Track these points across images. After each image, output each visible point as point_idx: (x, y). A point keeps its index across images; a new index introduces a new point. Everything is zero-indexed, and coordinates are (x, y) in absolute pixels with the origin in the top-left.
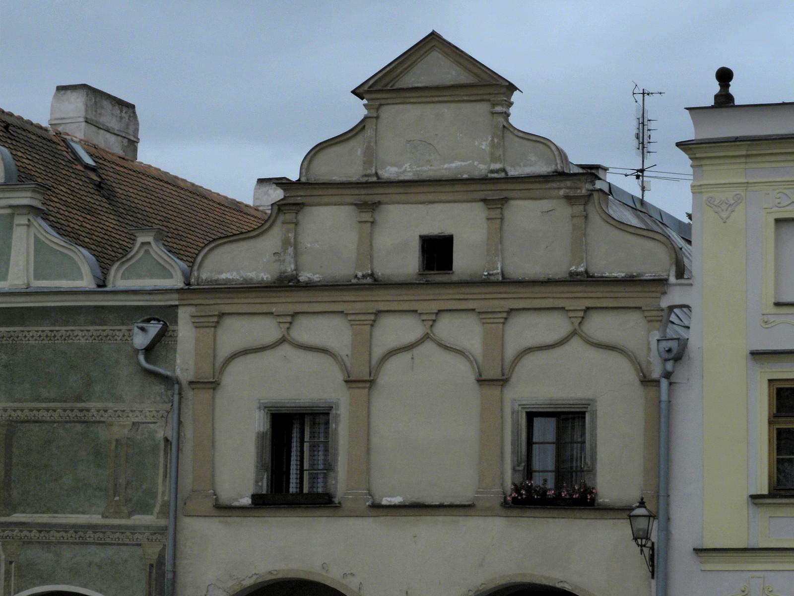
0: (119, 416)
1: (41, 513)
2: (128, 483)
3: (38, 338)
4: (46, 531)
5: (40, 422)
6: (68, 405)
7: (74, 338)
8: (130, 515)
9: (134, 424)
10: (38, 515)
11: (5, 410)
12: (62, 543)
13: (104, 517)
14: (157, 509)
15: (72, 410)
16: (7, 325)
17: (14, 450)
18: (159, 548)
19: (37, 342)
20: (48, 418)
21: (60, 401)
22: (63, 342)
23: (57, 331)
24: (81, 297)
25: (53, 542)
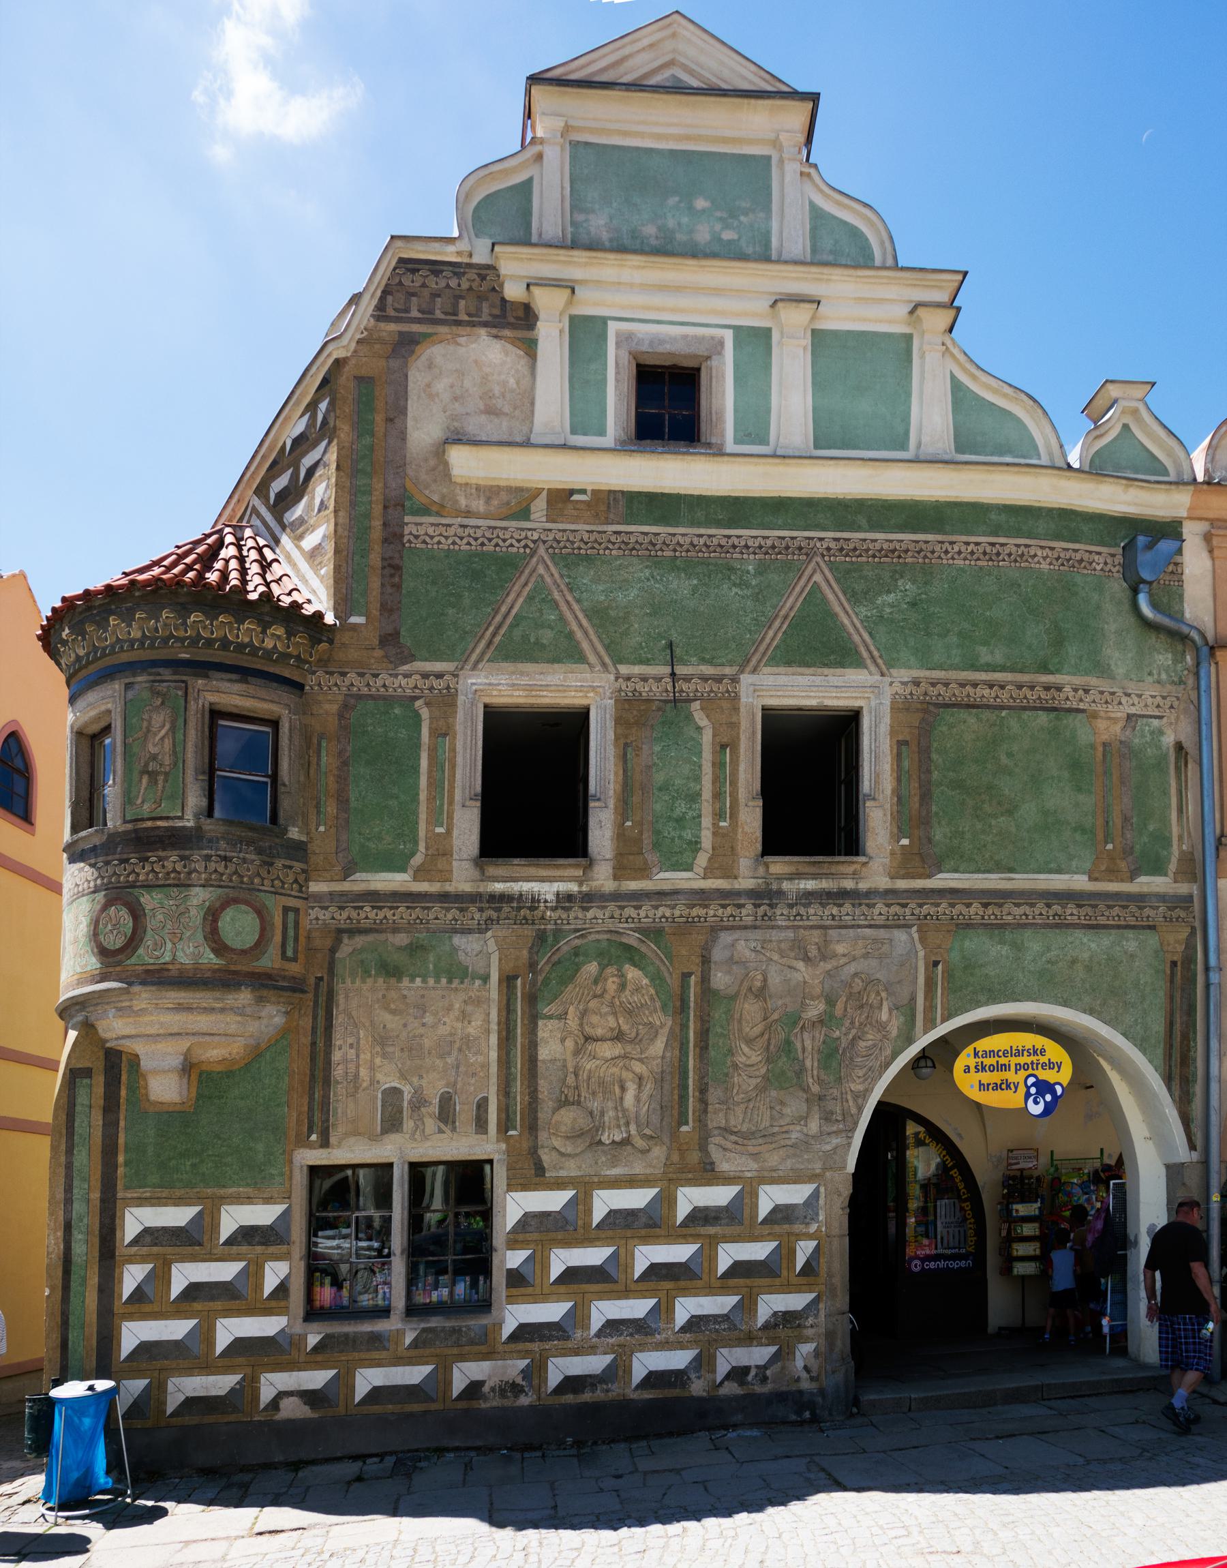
0: (1107, 702)
1: (984, 872)
2: (1126, 819)
4: (995, 904)
5: (978, 707)
6: (1025, 678)
8: (1133, 876)
9: (1129, 717)
10: (981, 876)
11: (917, 683)
12: (1024, 926)
13: (1091, 879)
14: (1173, 867)
15: (1032, 688)
17: (934, 756)
18: (1184, 934)
21: (1012, 670)
25: (1009, 924)
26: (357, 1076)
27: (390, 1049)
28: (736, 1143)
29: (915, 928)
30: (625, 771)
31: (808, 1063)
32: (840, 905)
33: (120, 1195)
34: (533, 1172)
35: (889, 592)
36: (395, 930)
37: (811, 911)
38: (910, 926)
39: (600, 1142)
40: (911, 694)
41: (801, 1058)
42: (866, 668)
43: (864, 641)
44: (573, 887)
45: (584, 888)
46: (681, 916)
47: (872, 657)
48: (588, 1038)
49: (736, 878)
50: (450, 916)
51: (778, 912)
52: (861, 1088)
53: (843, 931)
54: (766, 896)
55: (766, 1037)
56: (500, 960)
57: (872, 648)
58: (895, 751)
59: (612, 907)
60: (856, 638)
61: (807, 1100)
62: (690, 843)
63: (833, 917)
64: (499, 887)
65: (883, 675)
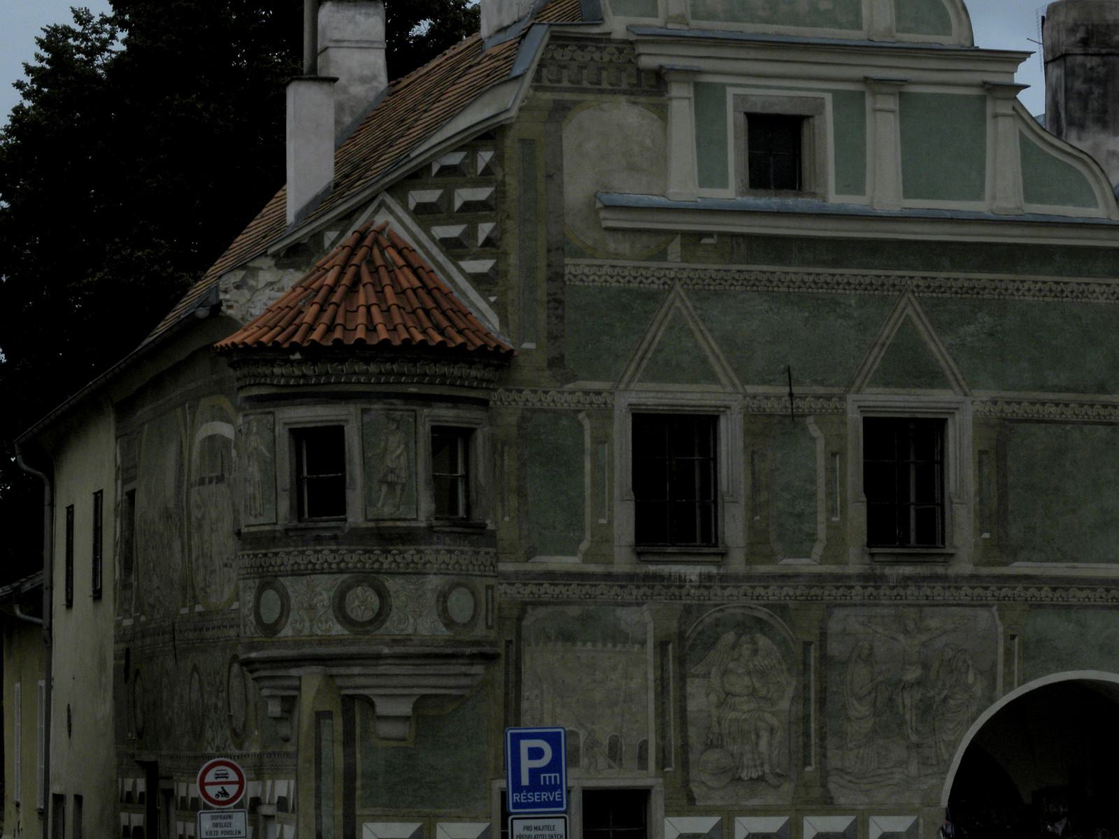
3: (1037, 293)
4: (1063, 588)
5: (1047, 422)
6: (1086, 398)
7: (1089, 296)
10: (1050, 564)
11: (995, 403)
12: (1086, 607)
15: (1092, 406)
16: (991, 270)
19: (1036, 299)
20: (1058, 416)
21: (1075, 390)
22: (1075, 300)
23: (1066, 283)
24: (1103, 234)
25: (1075, 606)
28: (850, 781)
29: (995, 608)
30: (753, 473)
31: (908, 717)
32: (933, 588)
33: (358, 812)
34: (686, 801)
35: (969, 323)
36: (569, 603)
37: (909, 592)
38: (992, 606)
39: (740, 779)
40: (990, 411)
41: (901, 713)
42: (952, 388)
43: (949, 366)
44: (713, 570)
45: (722, 571)
46: (802, 595)
47: (957, 380)
48: (728, 694)
49: (847, 564)
50: (613, 592)
51: (882, 592)
52: (952, 738)
53: (936, 609)
54: (868, 579)
55: (873, 695)
56: (655, 628)
57: (956, 371)
58: (977, 459)
59: (745, 587)
60: (942, 363)
61: (907, 747)
62: (808, 535)
63: (927, 597)
64: (652, 568)
65: (966, 395)
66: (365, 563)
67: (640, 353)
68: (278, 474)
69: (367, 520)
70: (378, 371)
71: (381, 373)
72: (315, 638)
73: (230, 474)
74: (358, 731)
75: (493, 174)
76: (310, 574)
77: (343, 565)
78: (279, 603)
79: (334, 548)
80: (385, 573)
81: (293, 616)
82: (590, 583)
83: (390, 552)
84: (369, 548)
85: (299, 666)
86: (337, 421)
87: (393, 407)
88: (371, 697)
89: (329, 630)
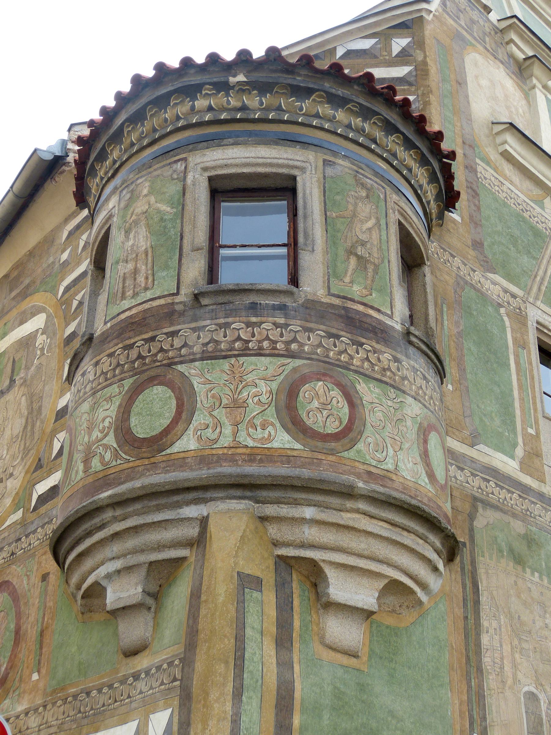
26: (502, 668)
27: (525, 645)
36: (514, 516)
66: (328, 350)
67: (538, 278)
68: (187, 229)
69: (330, 294)
70: (346, 122)
71: (349, 126)
72: (244, 450)
73: (27, 368)
74: (297, 623)
75: (411, 56)
76: (236, 356)
77: (294, 346)
78: (174, 402)
79: (282, 321)
80: (356, 372)
81: (199, 419)
82: (530, 498)
83: (362, 345)
84: (334, 331)
85: (205, 501)
86: (288, 166)
87: (360, 171)
88: (322, 564)
89: (269, 439)
